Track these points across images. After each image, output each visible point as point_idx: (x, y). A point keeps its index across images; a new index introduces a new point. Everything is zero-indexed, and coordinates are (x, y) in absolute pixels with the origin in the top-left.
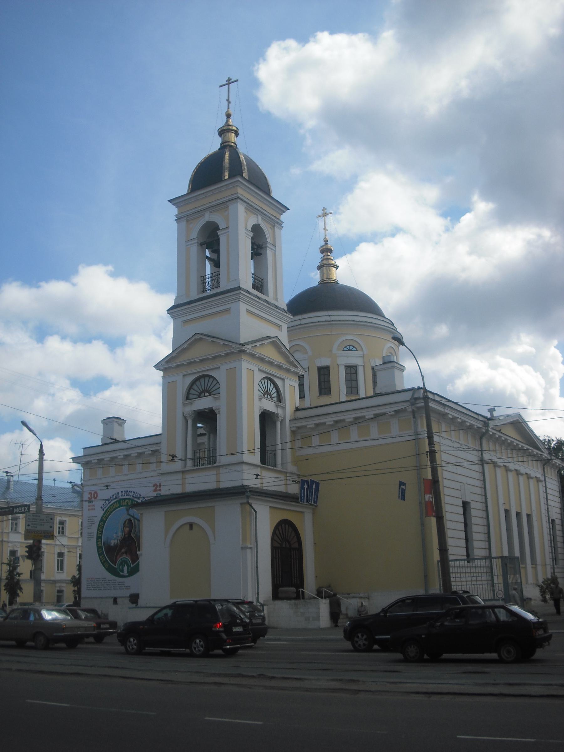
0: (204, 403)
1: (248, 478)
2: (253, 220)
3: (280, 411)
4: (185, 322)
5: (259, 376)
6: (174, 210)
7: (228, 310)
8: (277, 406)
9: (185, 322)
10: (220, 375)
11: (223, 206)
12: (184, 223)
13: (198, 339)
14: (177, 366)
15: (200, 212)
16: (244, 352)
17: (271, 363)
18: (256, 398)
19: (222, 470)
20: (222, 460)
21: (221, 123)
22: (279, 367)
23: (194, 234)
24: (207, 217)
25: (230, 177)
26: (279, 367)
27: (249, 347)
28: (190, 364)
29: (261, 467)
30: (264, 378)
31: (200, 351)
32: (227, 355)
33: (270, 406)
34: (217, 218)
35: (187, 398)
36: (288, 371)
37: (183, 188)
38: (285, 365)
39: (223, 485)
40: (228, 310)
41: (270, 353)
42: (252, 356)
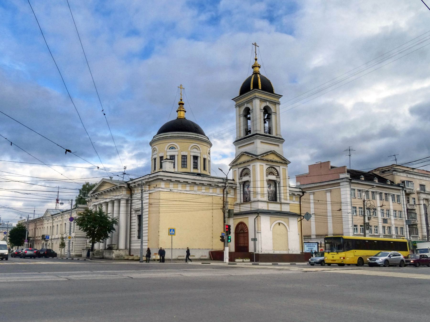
0: (245, 179)
1: (262, 206)
2: (264, 105)
3: (278, 180)
4: (239, 147)
5: (265, 167)
6: (235, 103)
7: (254, 142)
8: (277, 177)
9: (239, 147)
10: (251, 168)
11: (250, 101)
12: (238, 108)
13: (242, 154)
14: (236, 165)
15: (243, 104)
16: (258, 159)
17: (272, 161)
18: (265, 175)
19: (253, 204)
20: (252, 199)
21: (253, 62)
22: (277, 162)
23: (242, 112)
24: (246, 106)
25: (254, 88)
26: (277, 162)
27: (260, 156)
28: (240, 164)
29: (268, 202)
30: (269, 167)
31: (244, 158)
32: (252, 160)
33: (273, 177)
34: (249, 106)
35: (241, 176)
36: (282, 163)
37: (237, 93)
38: (281, 161)
39: (252, 209)
40: (254, 142)
41: (271, 157)
42: (263, 160)
